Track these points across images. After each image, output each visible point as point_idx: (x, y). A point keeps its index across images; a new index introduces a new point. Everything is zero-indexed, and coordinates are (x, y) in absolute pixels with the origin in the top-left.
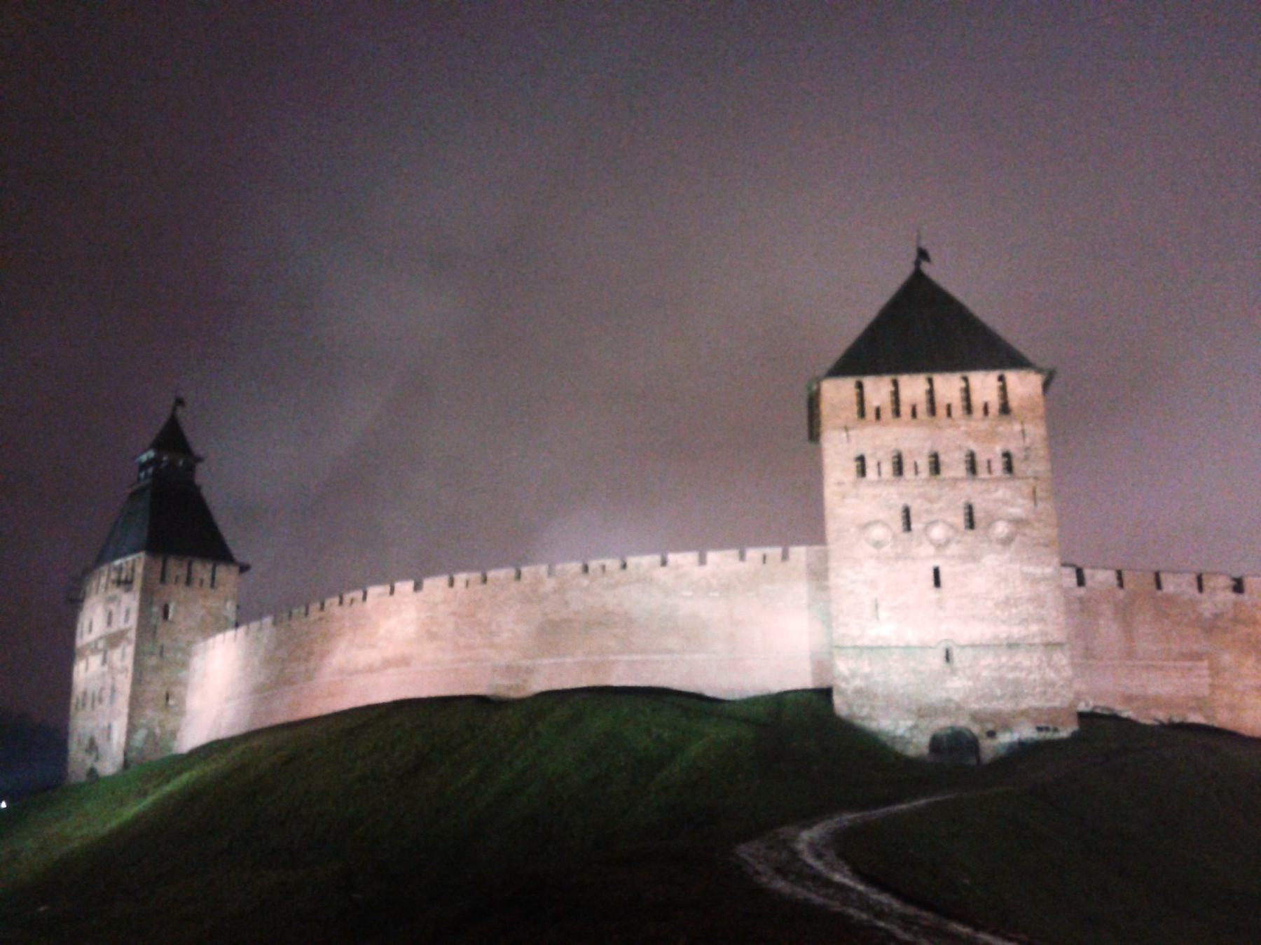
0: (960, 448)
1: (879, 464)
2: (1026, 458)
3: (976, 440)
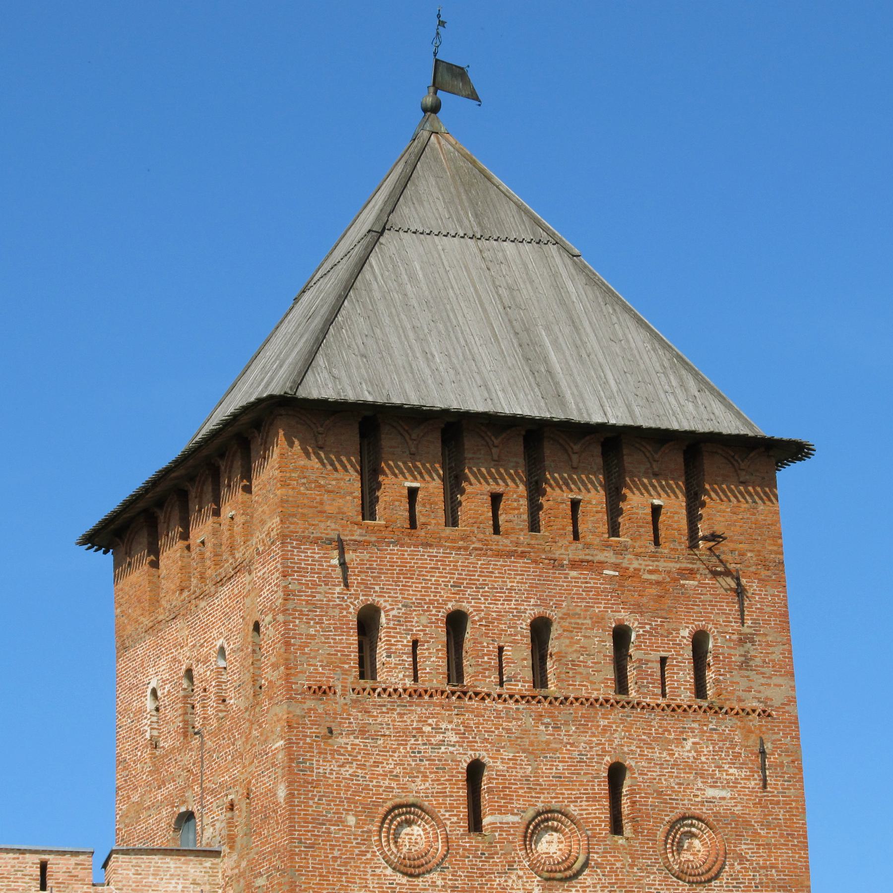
0: (599, 620)
1: (415, 643)
2: (746, 663)
3: (638, 609)
